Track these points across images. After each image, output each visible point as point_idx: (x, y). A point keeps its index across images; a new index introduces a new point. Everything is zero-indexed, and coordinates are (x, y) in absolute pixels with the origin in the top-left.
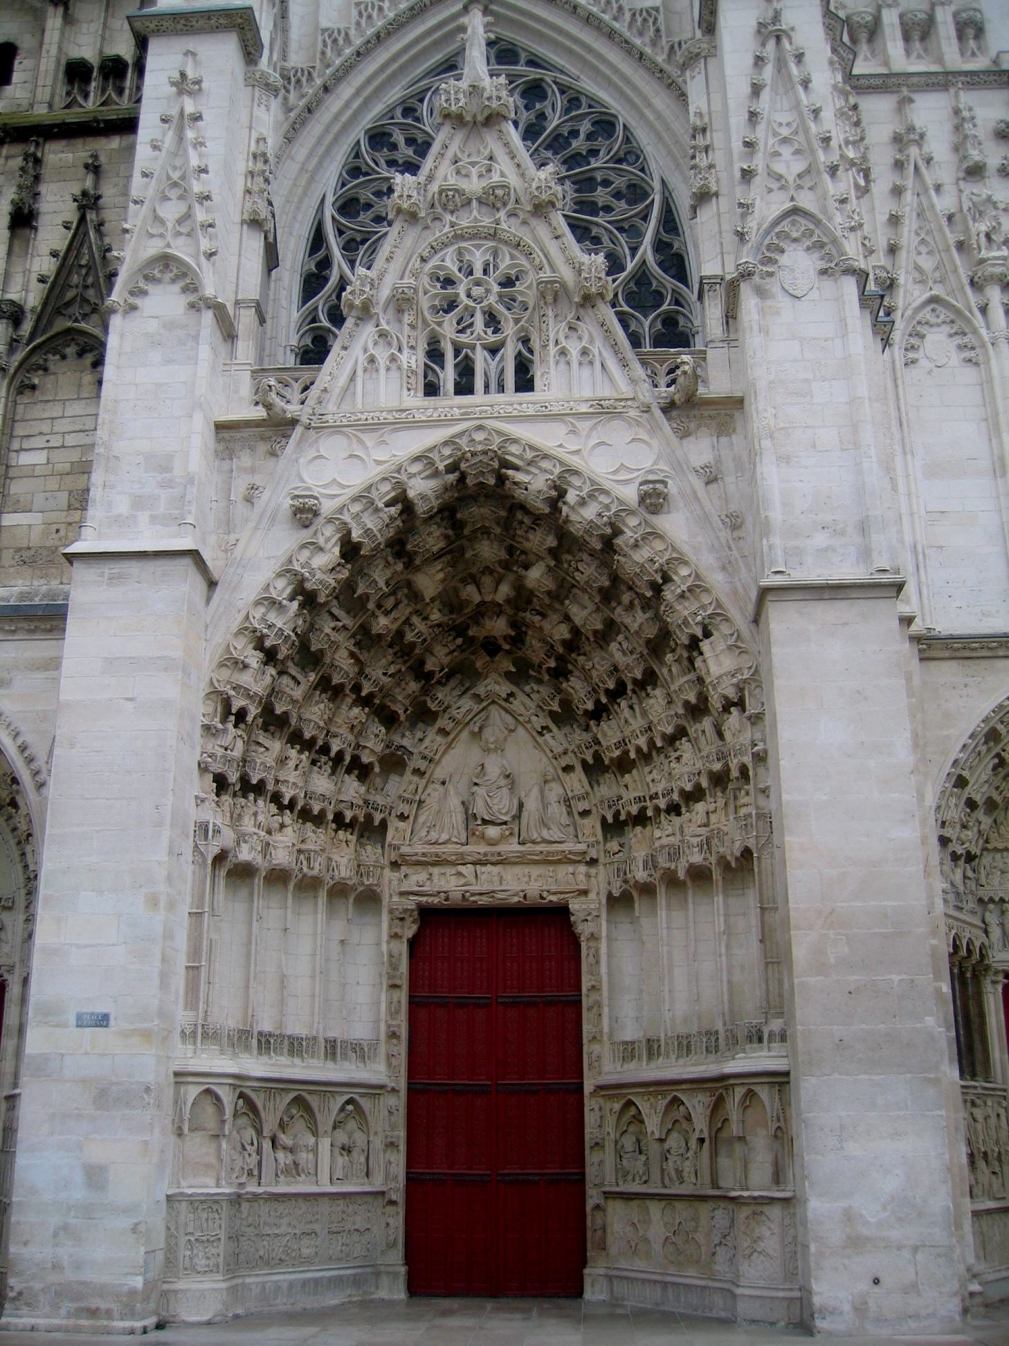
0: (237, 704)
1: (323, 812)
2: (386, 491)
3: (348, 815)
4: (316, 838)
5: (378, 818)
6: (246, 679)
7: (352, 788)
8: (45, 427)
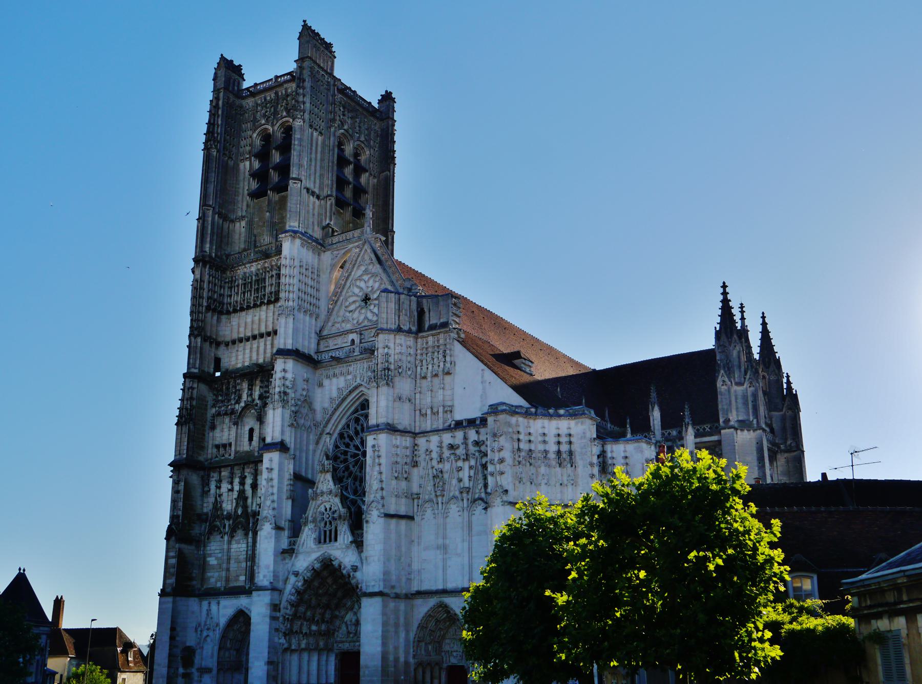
0: (287, 616)
1: (315, 634)
2: (311, 568)
3: (323, 633)
4: (312, 640)
5: (332, 631)
6: (288, 612)
7: (323, 627)
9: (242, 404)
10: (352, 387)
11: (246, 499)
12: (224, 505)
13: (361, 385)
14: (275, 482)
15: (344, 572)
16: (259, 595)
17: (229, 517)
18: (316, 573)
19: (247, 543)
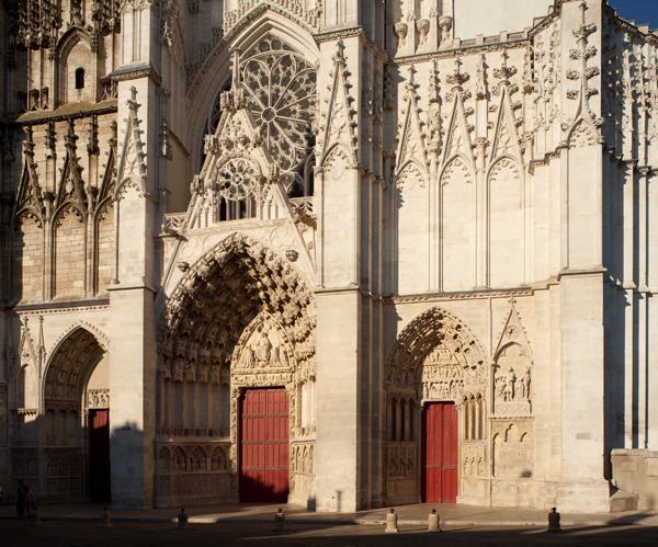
8: (108, 233)
9: (64, 29)
10: (251, 10)
11: (80, 170)
12: (41, 181)
13: (266, 8)
14: (144, 126)
15: (270, 264)
16: (122, 297)
17: (50, 197)
18: (216, 270)
19: (86, 232)
